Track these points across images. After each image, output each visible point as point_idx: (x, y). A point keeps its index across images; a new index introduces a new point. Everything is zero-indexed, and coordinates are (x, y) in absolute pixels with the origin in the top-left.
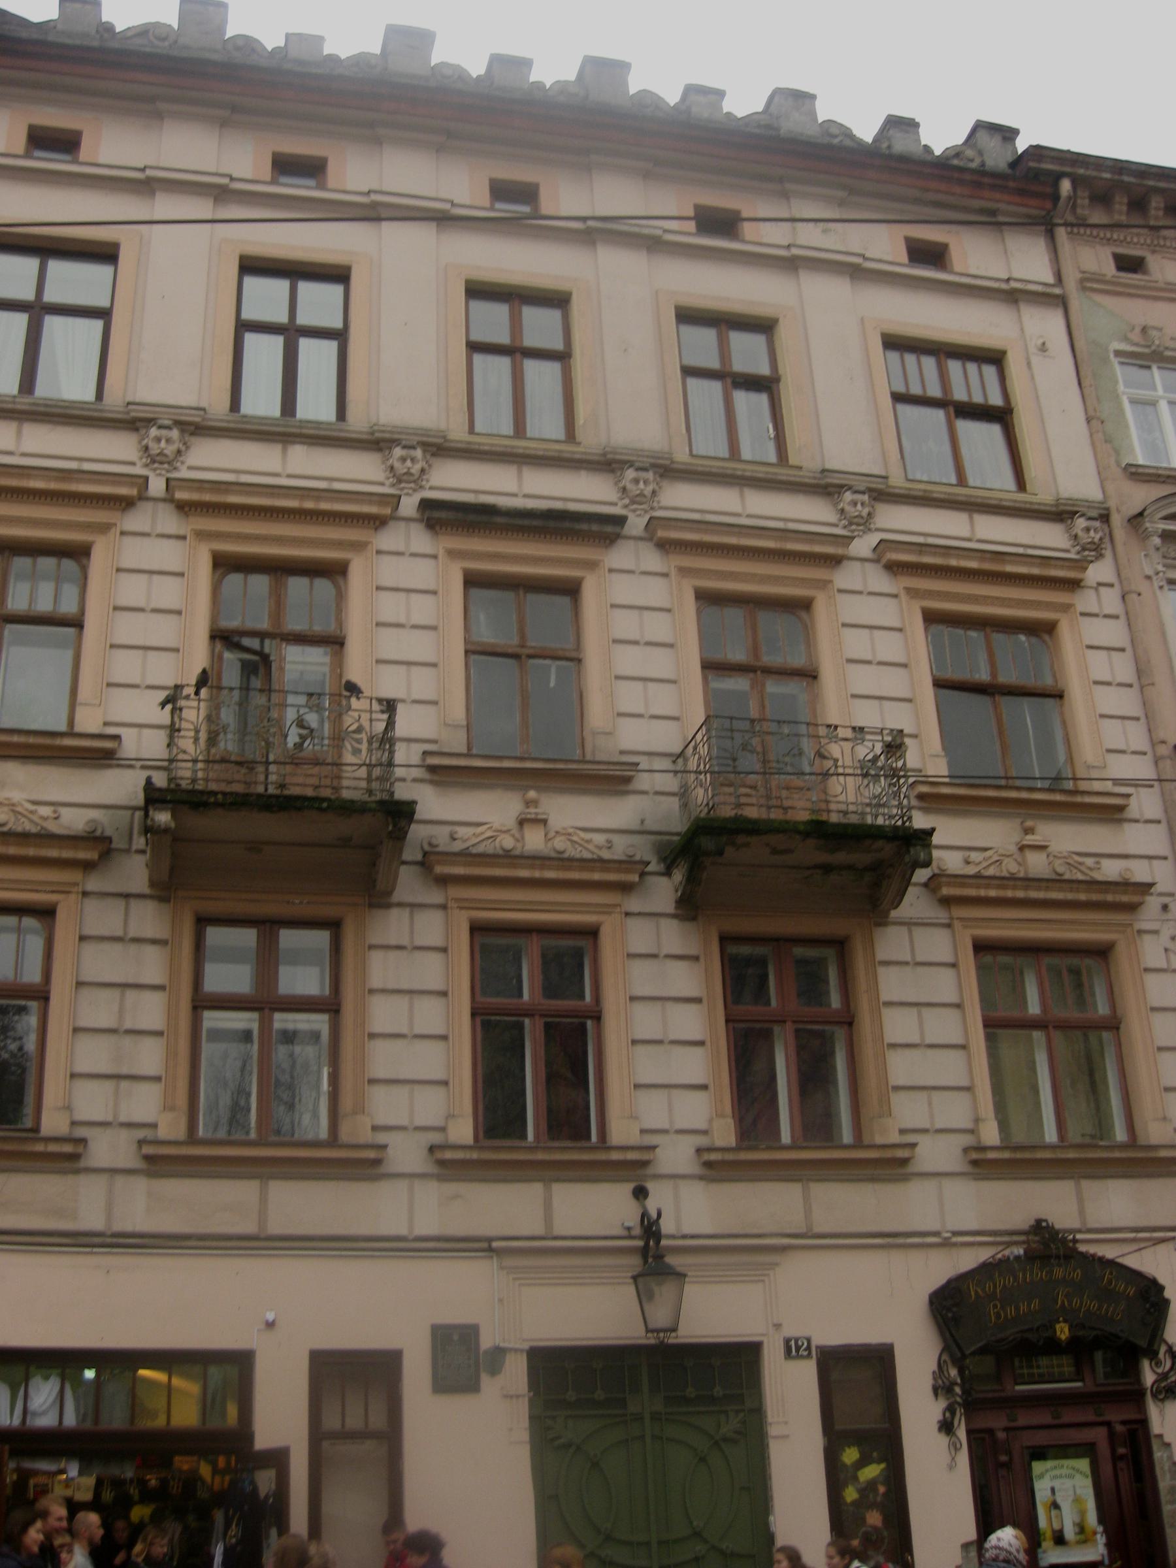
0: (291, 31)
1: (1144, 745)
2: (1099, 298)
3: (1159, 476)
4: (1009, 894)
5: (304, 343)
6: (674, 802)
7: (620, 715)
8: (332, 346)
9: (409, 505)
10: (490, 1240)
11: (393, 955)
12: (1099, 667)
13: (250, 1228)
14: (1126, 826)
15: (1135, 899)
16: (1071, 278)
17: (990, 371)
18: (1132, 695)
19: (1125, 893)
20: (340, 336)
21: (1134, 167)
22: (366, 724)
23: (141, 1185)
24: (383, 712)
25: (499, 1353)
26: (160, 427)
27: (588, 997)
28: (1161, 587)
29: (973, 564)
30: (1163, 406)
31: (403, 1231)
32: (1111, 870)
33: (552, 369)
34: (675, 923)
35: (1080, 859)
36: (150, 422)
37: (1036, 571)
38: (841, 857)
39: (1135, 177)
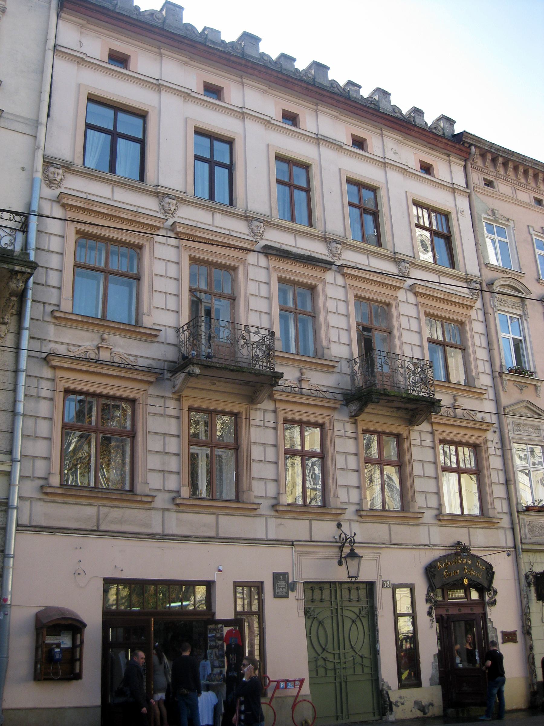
1: (488, 371)
3: (497, 269)
4: (452, 423)
6: (348, 378)
10: (292, 541)
11: (258, 429)
13: (213, 534)
15: (488, 428)
20: (230, 168)
21: (496, 147)
23: (174, 515)
25: (294, 583)
29: (442, 296)
31: (264, 537)
32: (479, 416)
39: (495, 150)
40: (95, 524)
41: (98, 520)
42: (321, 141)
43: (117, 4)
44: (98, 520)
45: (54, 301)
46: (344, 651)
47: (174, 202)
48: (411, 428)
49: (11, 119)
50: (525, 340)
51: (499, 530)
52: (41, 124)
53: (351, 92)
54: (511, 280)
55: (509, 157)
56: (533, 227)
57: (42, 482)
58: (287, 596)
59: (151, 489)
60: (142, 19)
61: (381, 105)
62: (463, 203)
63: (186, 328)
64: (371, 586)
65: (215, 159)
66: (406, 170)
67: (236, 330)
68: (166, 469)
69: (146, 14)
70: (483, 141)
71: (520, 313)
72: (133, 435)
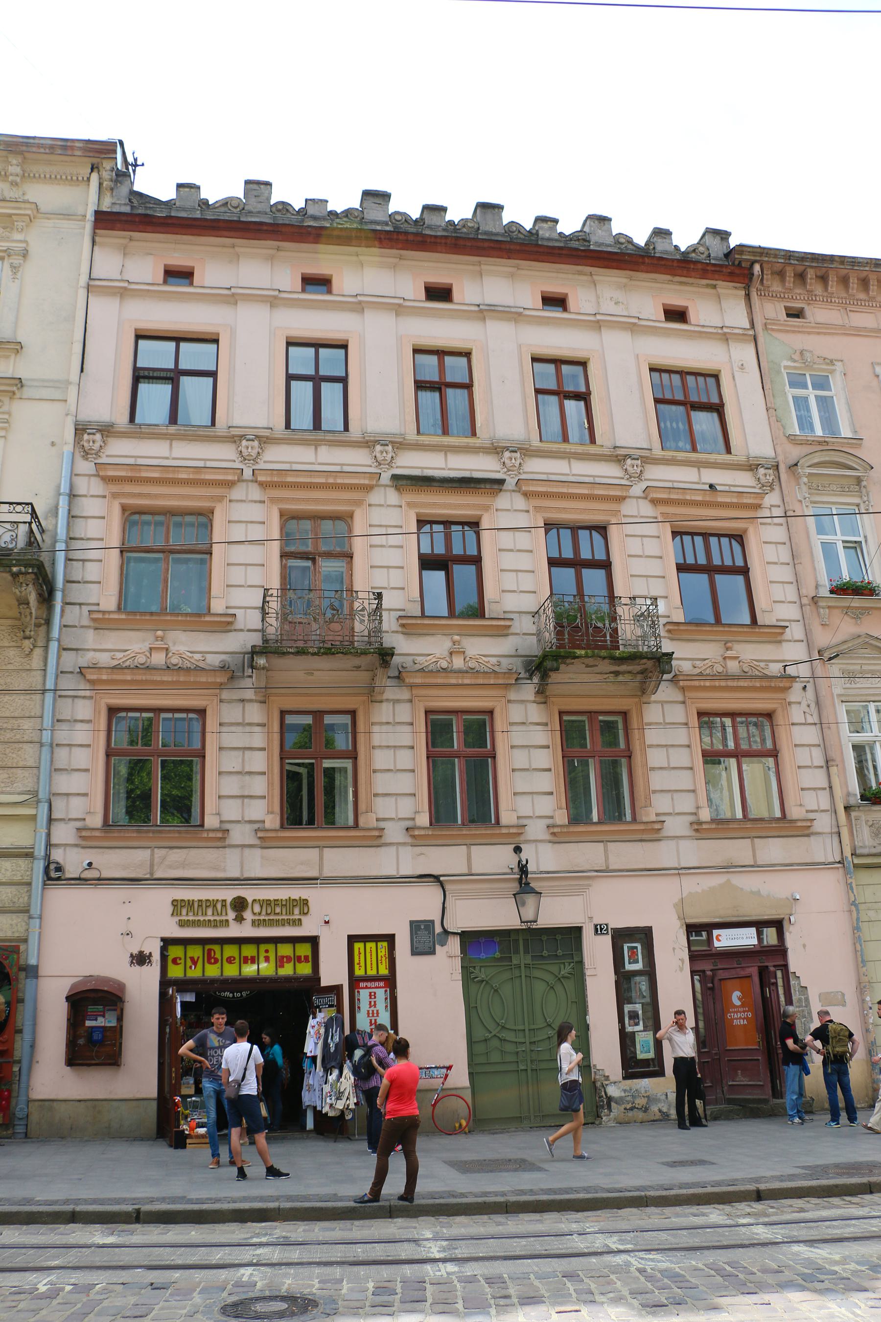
0: (309, 198)
1: (795, 598)
2: (774, 334)
4: (717, 683)
5: (325, 386)
7: (503, 591)
8: (339, 386)
9: (386, 478)
12: (771, 554)
13: (314, 873)
14: (784, 644)
15: (788, 685)
17: (711, 381)
19: (781, 682)
20: (343, 380)
21: (797, 255)
22: (367, 607)
23: (258, 852)
24: (375, 599)
27: (489, 747)
28: (807, 506)
31: (393, 873)
32: (775, 669)
33: (462, 393)
35: (757, 664)
36: (242, 437)
37: (735, 500)
38: (623, 668)
41: (152, 865)
42: (485, 313)
44: (152, 865)
46: (532, 1027)
48: (644, 699)
49: (37, 386)
50: (866, 541)
51: (812, 838)
53: (541, 233)
54: (832, 453)
55: (825, 265)
57: (79, 824)
58: (433, 952)
62: (745, 353)
68: (246, 794)
69: (217, 205)
70: (772, 252)
71: (856, 500)
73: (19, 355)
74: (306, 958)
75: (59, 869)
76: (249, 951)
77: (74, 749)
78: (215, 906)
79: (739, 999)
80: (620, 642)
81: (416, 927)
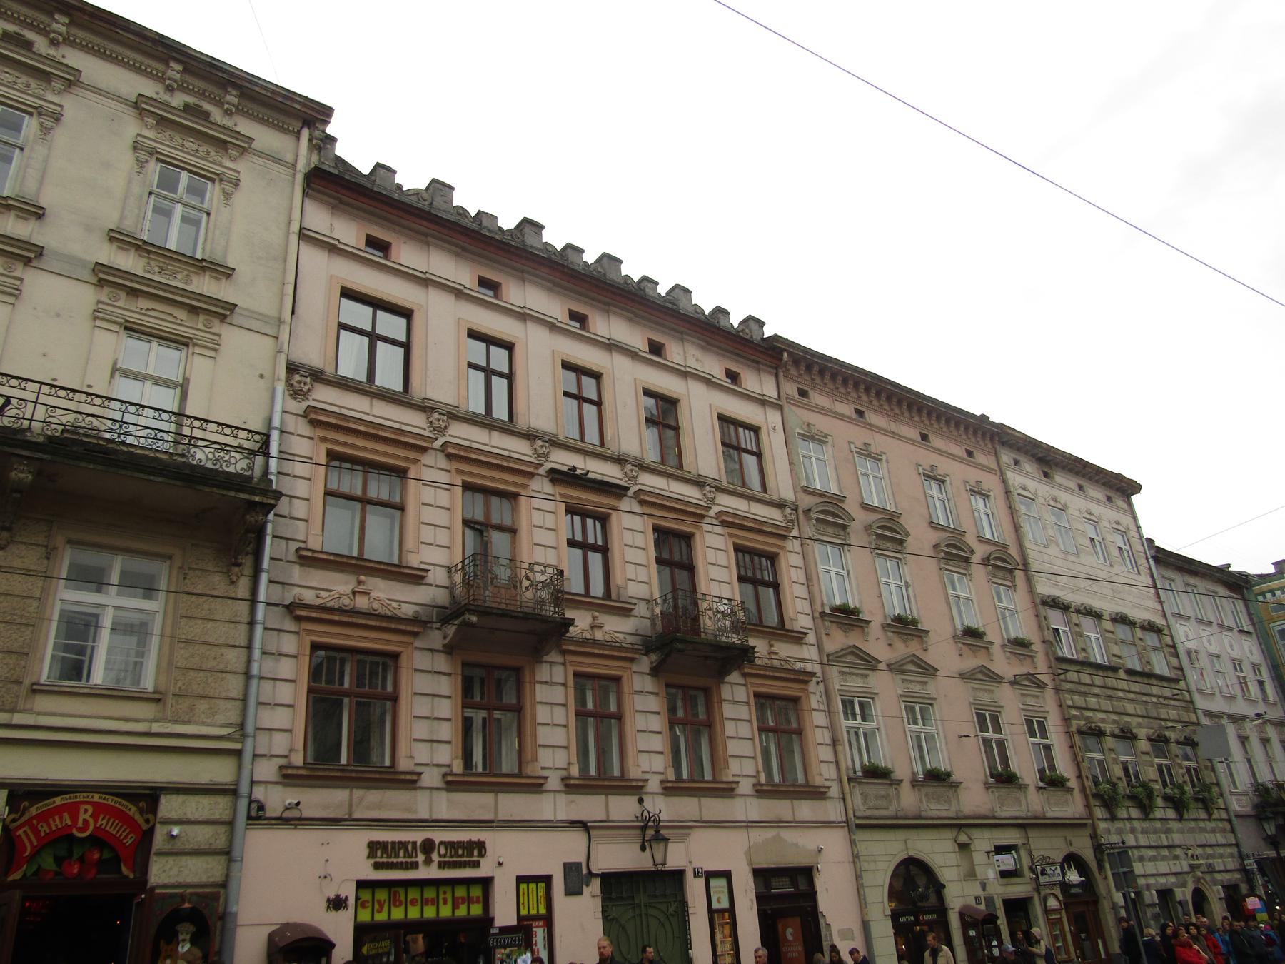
2: (793, 408)
4: (767, 673)
6: (648, 622)
11: (544, 686)
13: (488, 816)
16: (783, 396)
18: (804, 588)
20: (510, 377)
23: (444, 794)
26: (441, 414)
29: (752, 525)
30: (813, 459)
31: (552, 818)
32: (798, 666)
34: (649, 677)
36: (433, 409)
37: (774, 531)
40: (347, 811)
41: (351, 806)
43: (375, 181)
44: (351, 806)
45: (301, 537)
47: (445, 418)
52: (284, 322)
53: (647, 290)
54: (830, 505)
56: (853, 443)
57: (282, 762)
59: (416, 765)
60: (404, 199)
61: (681, 305)
62: (774, 417)
63: (460, 566)
64: (679, 875)
65: (492, 367)
66: (709, 380)
67: (518, 570)
68: (435, 738)
72: (394, 698)
73: (228, 280)
74: (478, 898)
75: (261, 807)
76: (430, 893)
77: (278, 682)
78: (406, 850)
79: (791, 934)
80: (702, 630)
81: (571, 869)
